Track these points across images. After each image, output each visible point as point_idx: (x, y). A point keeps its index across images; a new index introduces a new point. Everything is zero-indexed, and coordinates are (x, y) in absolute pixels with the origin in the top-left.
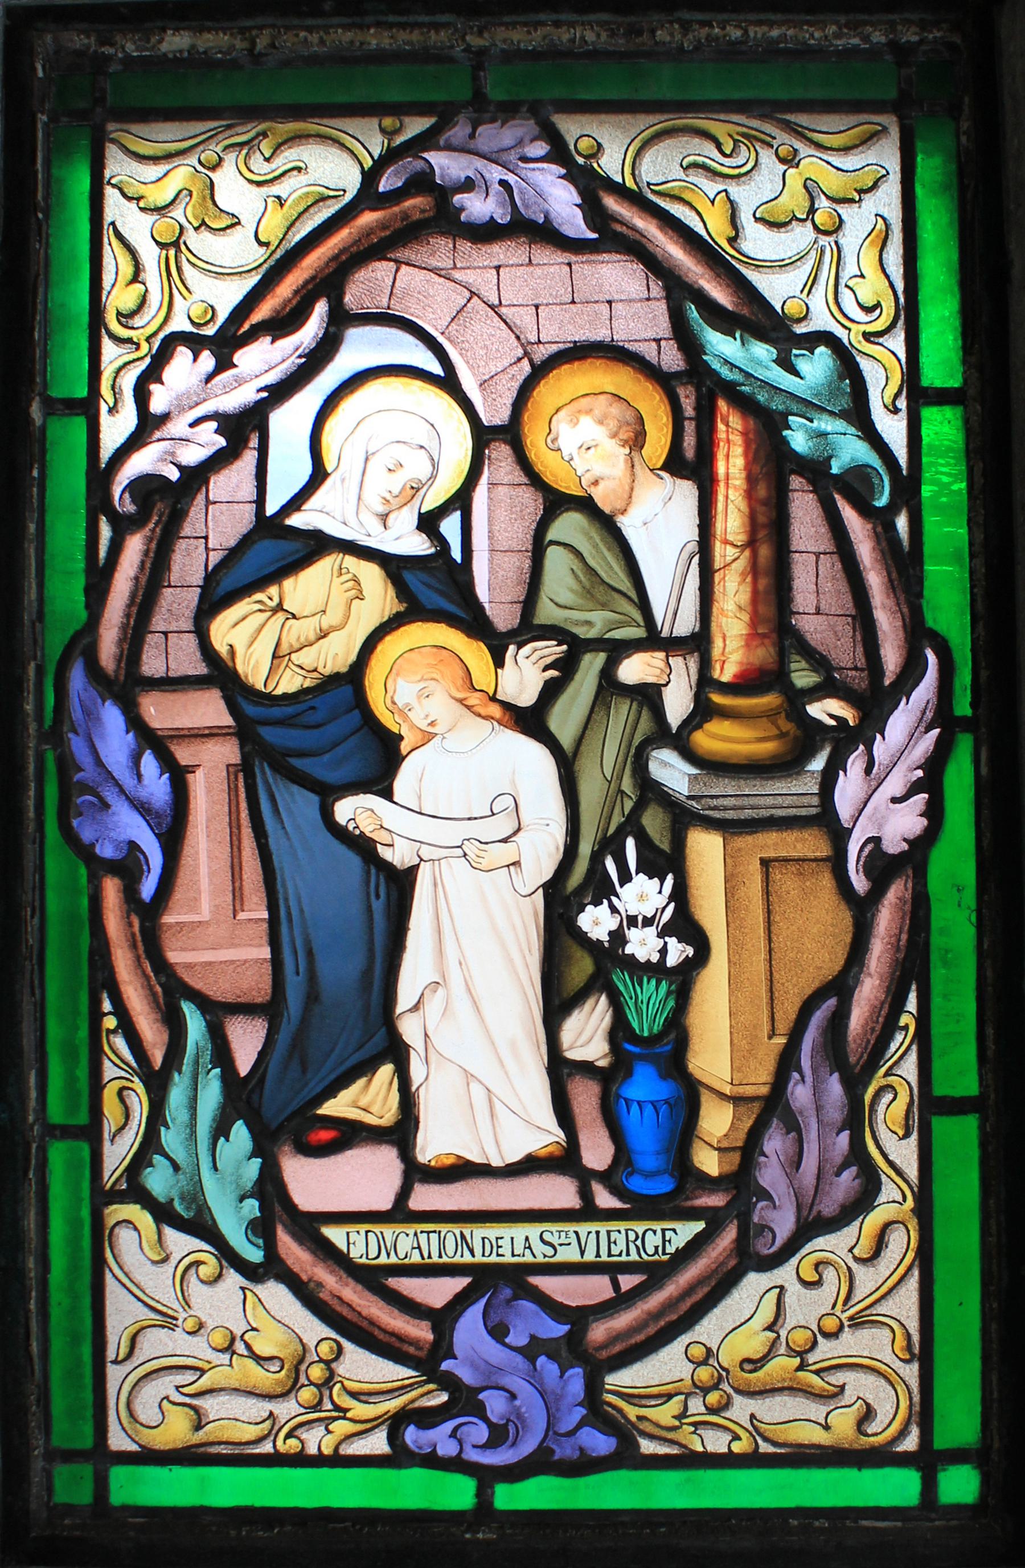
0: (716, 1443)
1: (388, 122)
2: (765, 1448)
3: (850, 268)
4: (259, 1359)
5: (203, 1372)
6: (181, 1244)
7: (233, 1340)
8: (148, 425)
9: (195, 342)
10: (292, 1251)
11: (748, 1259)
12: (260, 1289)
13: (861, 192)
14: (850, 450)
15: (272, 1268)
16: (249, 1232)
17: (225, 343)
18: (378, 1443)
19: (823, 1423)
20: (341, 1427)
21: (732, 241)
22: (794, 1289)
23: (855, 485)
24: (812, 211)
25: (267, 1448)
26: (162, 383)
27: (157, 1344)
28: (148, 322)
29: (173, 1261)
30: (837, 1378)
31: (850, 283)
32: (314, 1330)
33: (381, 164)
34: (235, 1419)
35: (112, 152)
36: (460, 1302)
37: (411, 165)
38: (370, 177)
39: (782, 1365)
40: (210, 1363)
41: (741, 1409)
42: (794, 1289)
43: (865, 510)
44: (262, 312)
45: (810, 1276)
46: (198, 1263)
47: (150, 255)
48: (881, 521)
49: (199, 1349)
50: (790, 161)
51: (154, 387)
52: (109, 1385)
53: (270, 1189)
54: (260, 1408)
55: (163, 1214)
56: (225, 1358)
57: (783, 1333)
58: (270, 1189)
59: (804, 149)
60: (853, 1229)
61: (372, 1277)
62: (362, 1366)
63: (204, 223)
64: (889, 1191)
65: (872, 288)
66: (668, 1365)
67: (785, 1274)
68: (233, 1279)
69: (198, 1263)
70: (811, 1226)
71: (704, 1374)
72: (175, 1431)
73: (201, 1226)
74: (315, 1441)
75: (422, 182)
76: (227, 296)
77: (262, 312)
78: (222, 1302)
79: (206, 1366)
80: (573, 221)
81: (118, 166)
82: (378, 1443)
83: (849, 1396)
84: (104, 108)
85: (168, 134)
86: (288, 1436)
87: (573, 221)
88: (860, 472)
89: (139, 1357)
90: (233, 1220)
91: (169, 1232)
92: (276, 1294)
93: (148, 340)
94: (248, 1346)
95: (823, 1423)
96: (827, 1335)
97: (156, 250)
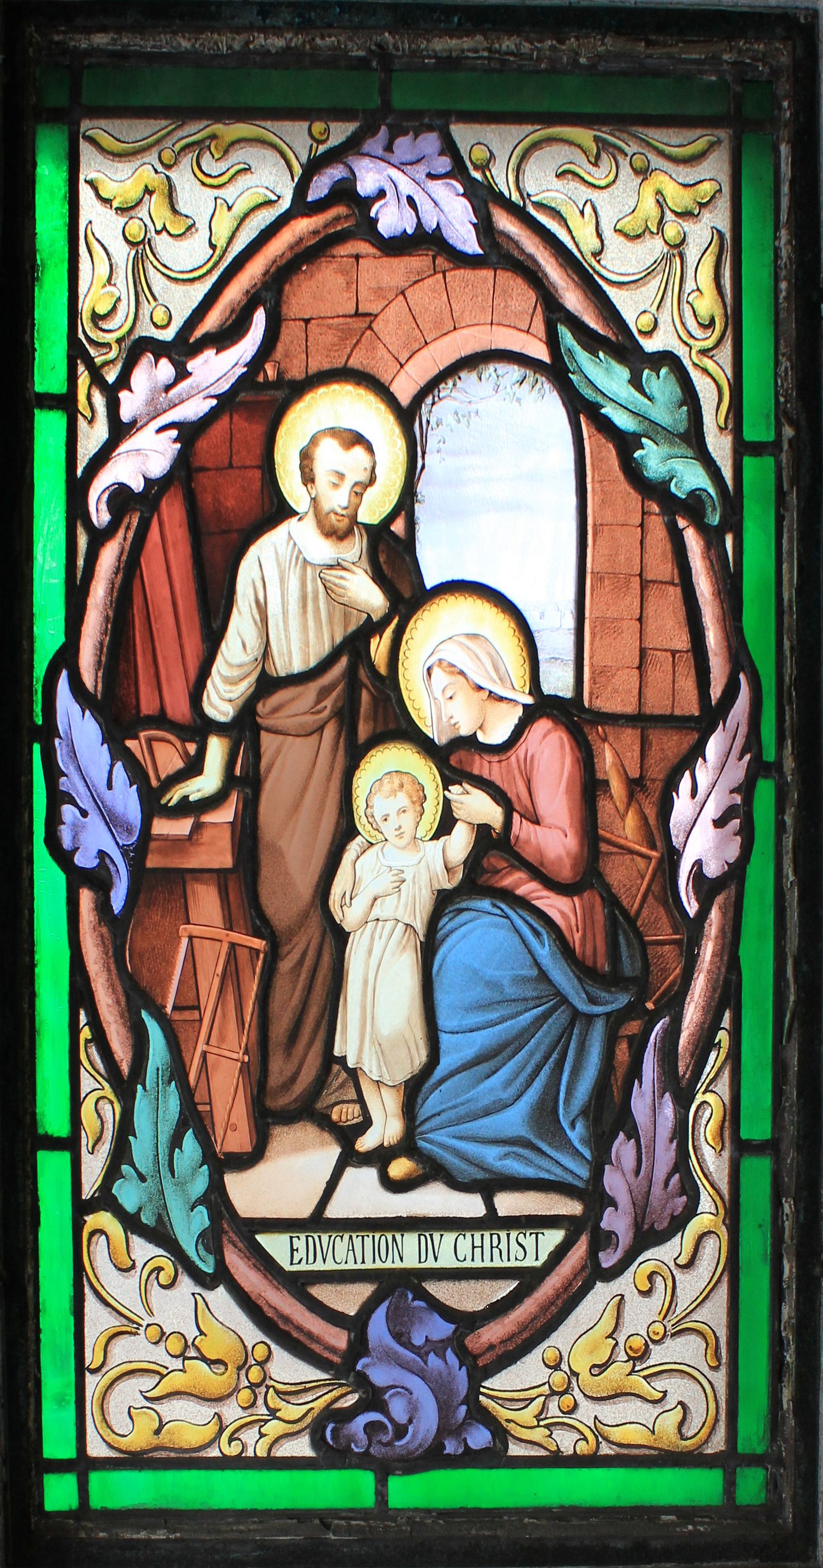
0: (566, 1442)
1: (318, 127)
2: (606, 1450)
3: (690, 285)
4: (210, 1362)
5: (163, 1376)
6: (144, 1250)
7: (186, 1346)
8: (120, 430)
9: (159, 349)
10: (235, 1260)
11: (595, 1273)
12: (210, 1296)
13: (702, 206)
14: (690, 477)
15: (220, 1276)
16: (200, 1247)
17: (182, 349)
18: (302, 1447)
19: (651, 1427)
20: (274, 1428)
21: (596, 254)
22: (632, 1298)
23: (693, 506)
24: (661, 223)
25: (214, 1453)
26: (131, 391)
27: (124, 1351)
28: (119, 323)
29: (139, 1269)
30: (660, 1384)
31: (690, 299)
32: (252, 1334)
33: (313, 167)
34: (189, 1423)
35: (86, 150)
36: (368, 1309)
37: (336, 172)
38: (301, 190)
39: (617, 1371)
40: (167, 1368)
41: (587, 1412)
42: (632, 1298)
43: (702, 528)
44: (212, 321)
45: (645, 1286)
46: (160, 1269)
47: (122, 253)
48: (712, 539)
49: (159, 1355)
50: (643, 173)
51: (123, 395)
52: (87, 1390)
53: (216, 1200)
54: (206, 1412)
55: (131, 1223)
56: (178, 1364)
57: (621, 1340)
58: (216, 1200)
59: (656, 161)
60: (677, 1239)
61: (298, 1284)
62: (287, 1368)
63: (164, 228)
64: (706, 1203)
65: (707, 304)
66: (528, 1373)
67: (624, 1284)
68: (186, 1284)
69: (160, 1269)
70: (647, 1237)
71: (558, 1378)
72: (138, 1437)
73: (161, 1235)
74: (254, 1444)
75: (344, 192)
76: (182, 301)
77: (212, 321)
78: (176, 1307)
79: (165, 1372)
80: (465, 238)
81: (92, 166)
82: (302, 1447)
83: (671, 1401)
84: (80, 101)
85: (140, 130)
86: (231, 1440)
87: (465, 238)
88: (696, 498)
89: (111, 1363)
90: (189, 1226)
91: (135, 1240)
92: (220, 1298)
93: (119, 341)
94: (198, 1349)
95: (651, 1427)
96: (655, 1342)
97: (126, 248)
